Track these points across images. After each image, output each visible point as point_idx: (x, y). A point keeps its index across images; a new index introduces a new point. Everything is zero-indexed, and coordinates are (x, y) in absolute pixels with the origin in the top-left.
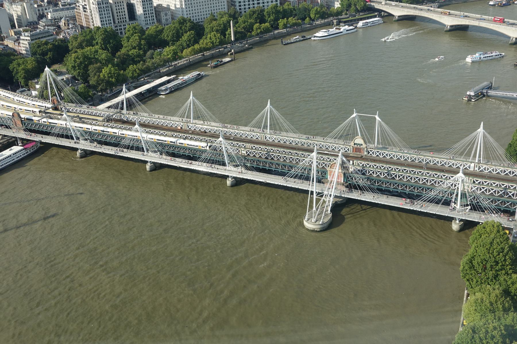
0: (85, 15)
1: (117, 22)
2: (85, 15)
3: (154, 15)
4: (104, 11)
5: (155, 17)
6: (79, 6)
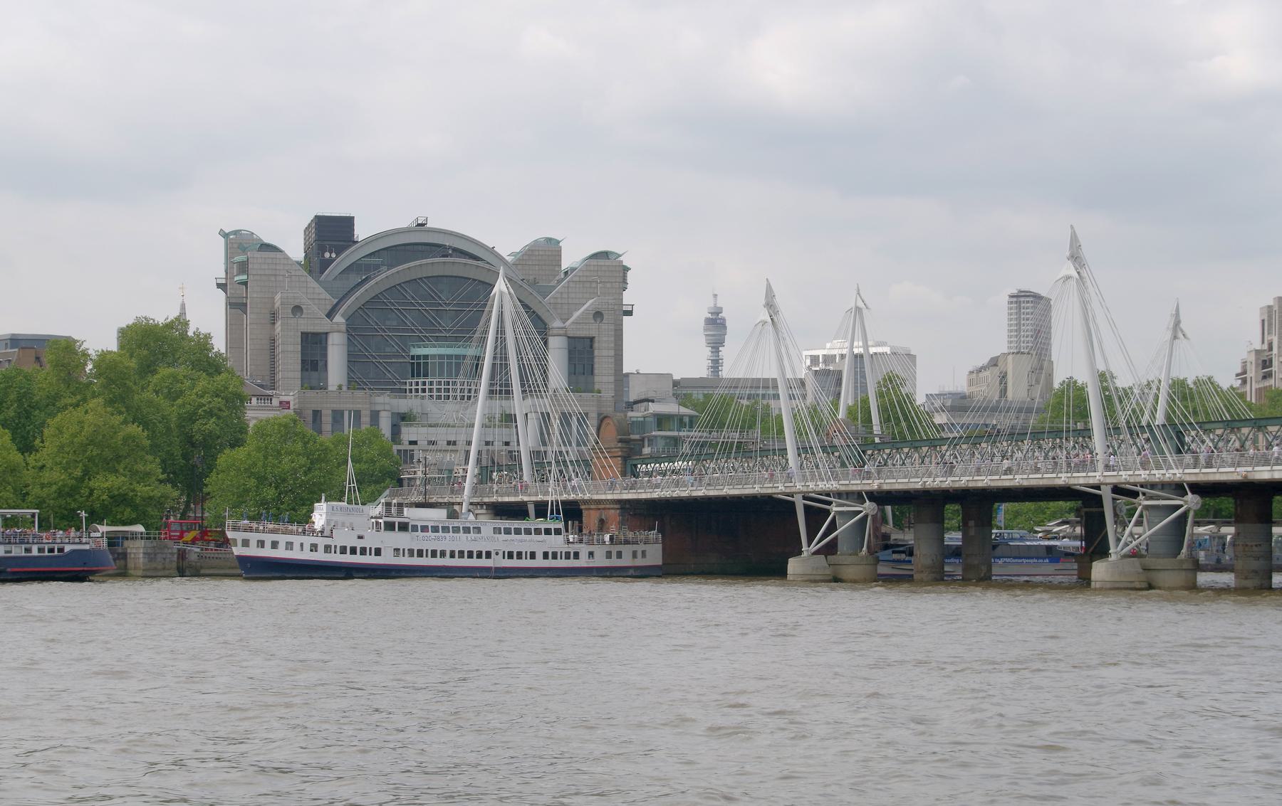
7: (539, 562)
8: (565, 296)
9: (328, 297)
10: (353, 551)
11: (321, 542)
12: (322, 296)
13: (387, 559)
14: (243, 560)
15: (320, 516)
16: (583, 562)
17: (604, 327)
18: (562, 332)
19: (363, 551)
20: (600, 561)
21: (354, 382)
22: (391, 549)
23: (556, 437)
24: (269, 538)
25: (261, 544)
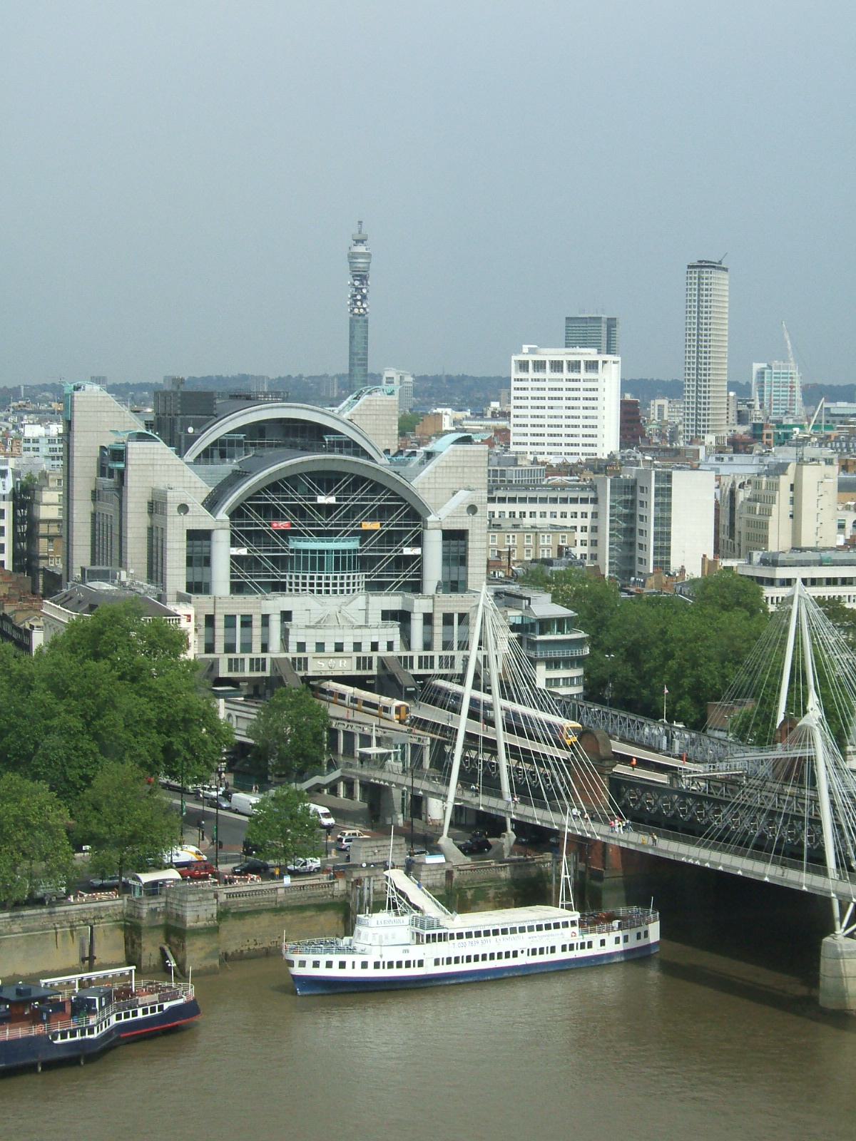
8: (432, 480)
9: (204, 485)
10: (399, 965)
12: (193, 480)
13: (430, 969)
17: (477, 519)
18: (436, 525)
19: (408, 964)
22: (430, 959)
23: (438, 642)
24: (323, 959)
25: (316, 964)
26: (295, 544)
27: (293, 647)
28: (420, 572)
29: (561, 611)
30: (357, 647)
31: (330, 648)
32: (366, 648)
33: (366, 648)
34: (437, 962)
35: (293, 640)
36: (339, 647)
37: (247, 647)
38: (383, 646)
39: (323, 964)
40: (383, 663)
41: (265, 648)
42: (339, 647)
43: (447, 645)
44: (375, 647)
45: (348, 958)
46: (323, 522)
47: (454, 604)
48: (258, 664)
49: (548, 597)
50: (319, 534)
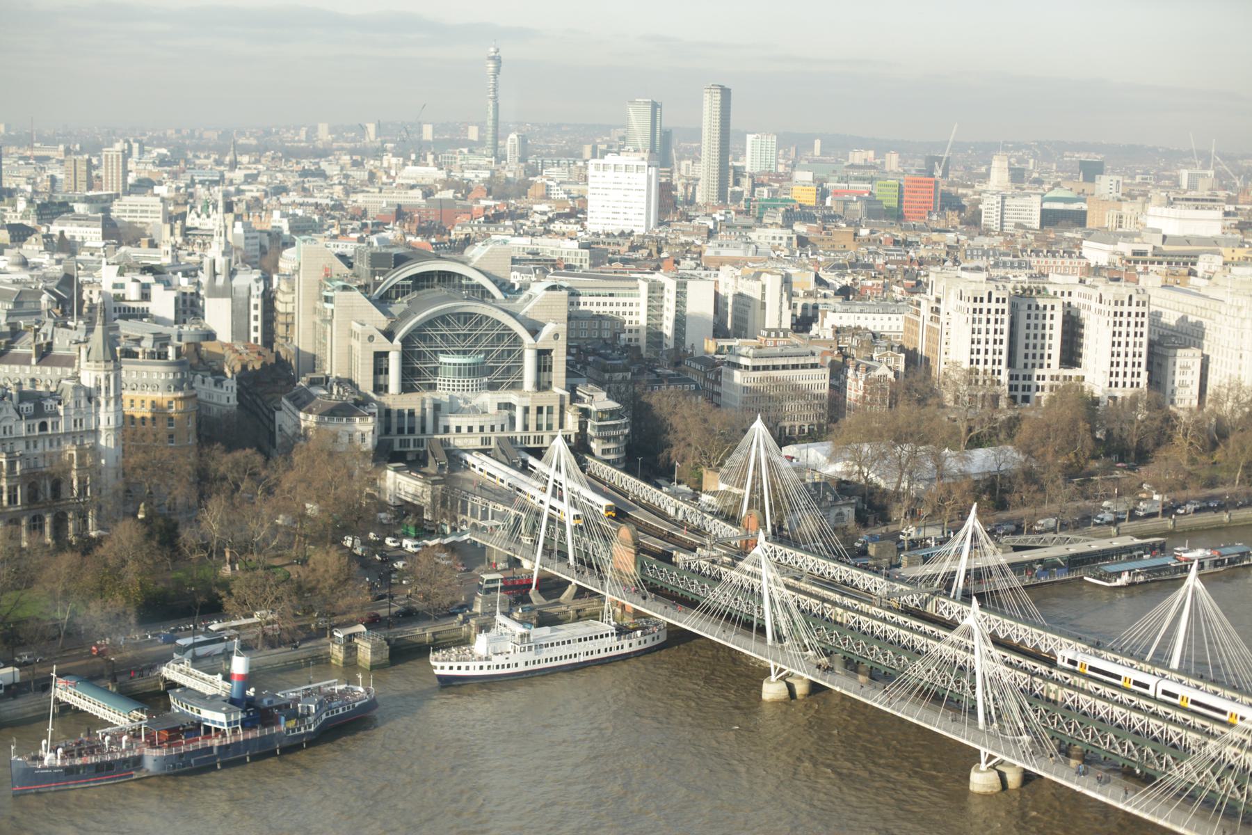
0: (930, 329)
1: (1020, 361)
2: (930, 329)
3: (1143, 360)
4: (988, 321)
5: (1143, 369)
6: (919, 304)
7: (603, 655)
11: (485, 664)
13: (522, 668)
14: (440, 677)
15: (481, 644)
16: (626, 650)
20: (635, 648)
21: (406, 388)
22: (520, 661)
23: (532, 426)
24: (455, 665)
25: (451, 668)
26: (443, 359)
27: (441, 429)
28: (521, 377)
29: (613, 405)
30: (482, 429)
31: (464, 430)
32: (487, 429)
33: (487, 429)
34: (527, 664)
35: (442, 423)
36: (470, 429)
37: (412, 431)
38: (497, 428)
39: (455, 668)
40: (499, 441)
41: (423, 430)
42: (470, 429)
43: (539, 427)
44: (492, 428)
45: (471, 664)
46: (464, 346)
47: (546, 399)
48: (419, 443)
49: (604, 394)
50: (458, 352)
